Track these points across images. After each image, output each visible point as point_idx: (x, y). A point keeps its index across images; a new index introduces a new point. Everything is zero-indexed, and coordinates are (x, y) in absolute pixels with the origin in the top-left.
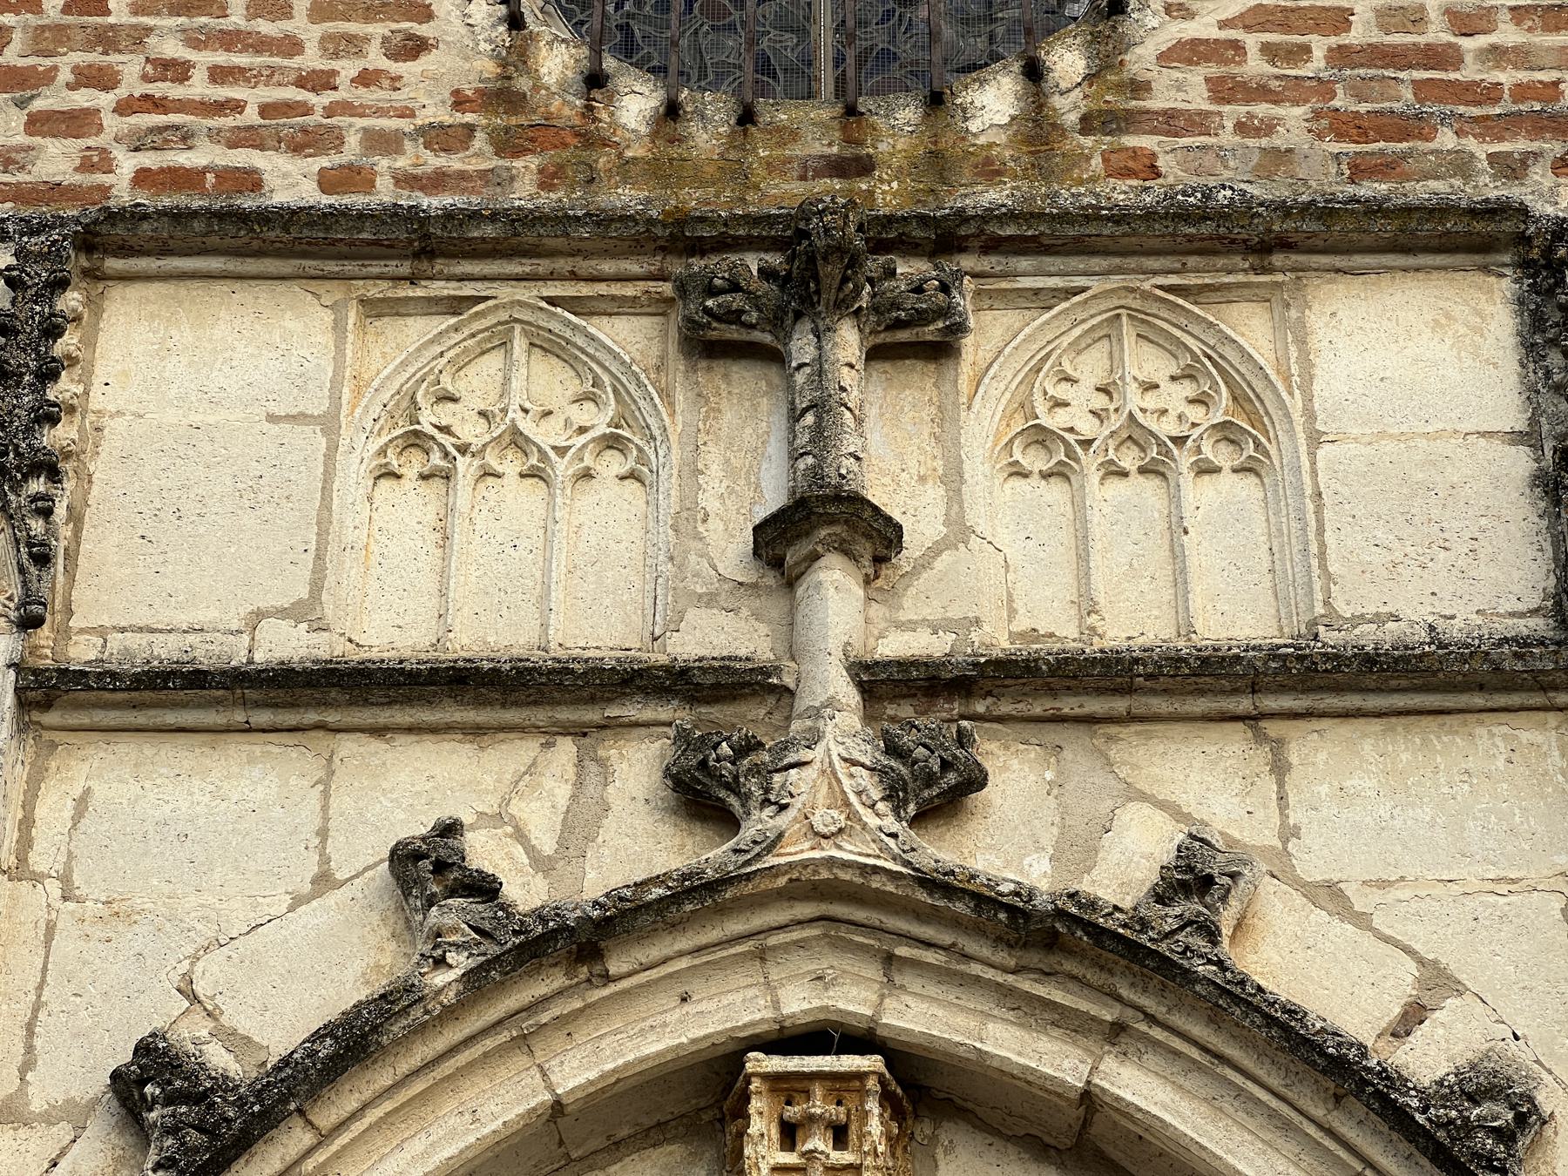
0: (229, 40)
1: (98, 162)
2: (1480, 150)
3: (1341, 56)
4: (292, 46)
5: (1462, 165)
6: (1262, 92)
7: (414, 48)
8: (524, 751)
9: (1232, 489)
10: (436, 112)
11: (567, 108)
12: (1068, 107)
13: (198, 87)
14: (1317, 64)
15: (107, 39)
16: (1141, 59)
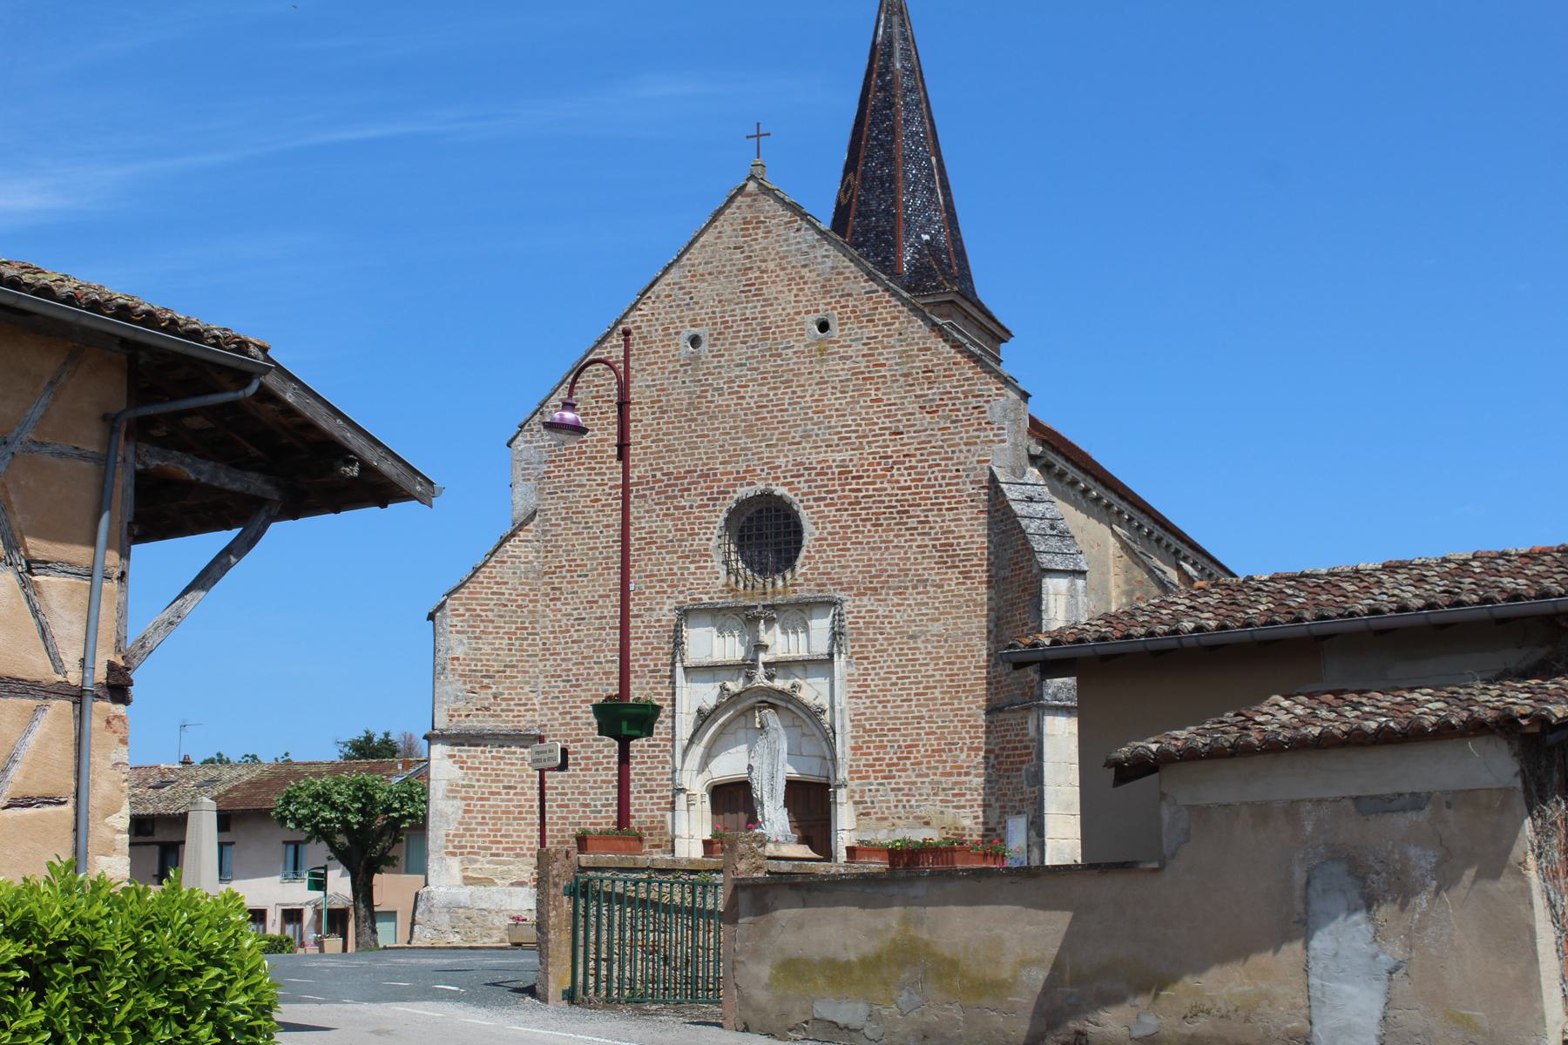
0: (698, 579)
1: (685, 598)
2: (832, 588)
3: (819, 574)
4: (704, 579)
5: (830, 590)
6: (809, 580)
7: (717, 578)
8: (732, 672)
9: (804, 635)
10: (720, 588)
11: (734, 586)
12: (789, 583)
13: (695, 586)
14: (815, 576)
15: (685, 580)
16: (797, 576)
